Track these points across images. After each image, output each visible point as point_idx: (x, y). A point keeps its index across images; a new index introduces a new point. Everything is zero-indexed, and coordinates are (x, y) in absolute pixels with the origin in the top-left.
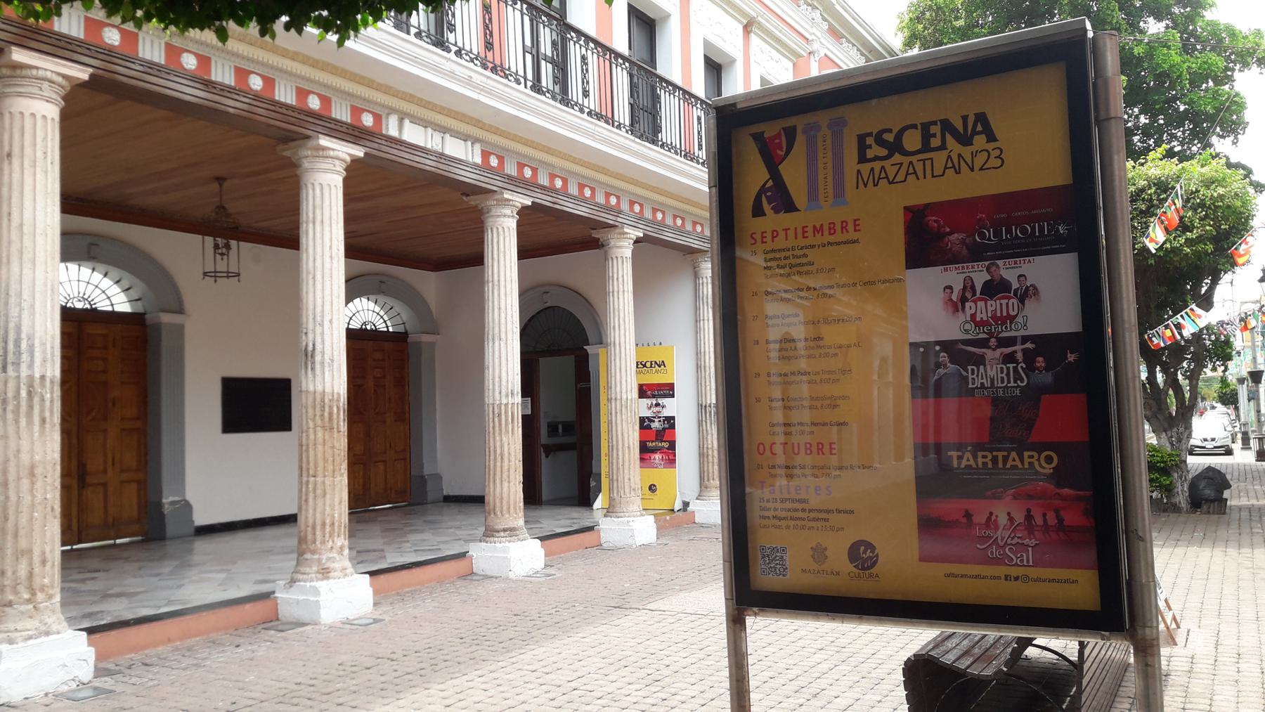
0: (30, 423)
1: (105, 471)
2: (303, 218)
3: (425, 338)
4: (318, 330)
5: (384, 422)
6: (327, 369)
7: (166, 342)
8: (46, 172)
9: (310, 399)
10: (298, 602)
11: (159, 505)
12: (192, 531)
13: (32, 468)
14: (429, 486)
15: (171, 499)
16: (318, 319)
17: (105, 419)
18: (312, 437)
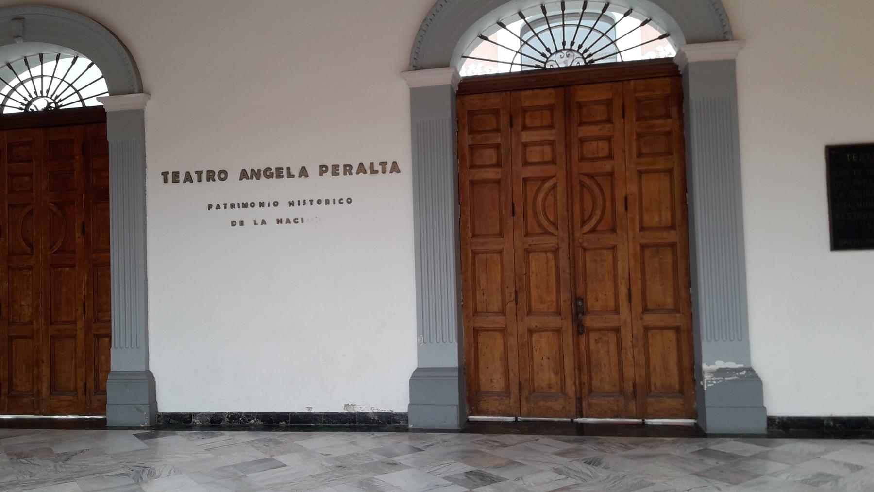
1: (617, 311)
12: (762, 427)
15: (720, 364)
17: (613, 230)
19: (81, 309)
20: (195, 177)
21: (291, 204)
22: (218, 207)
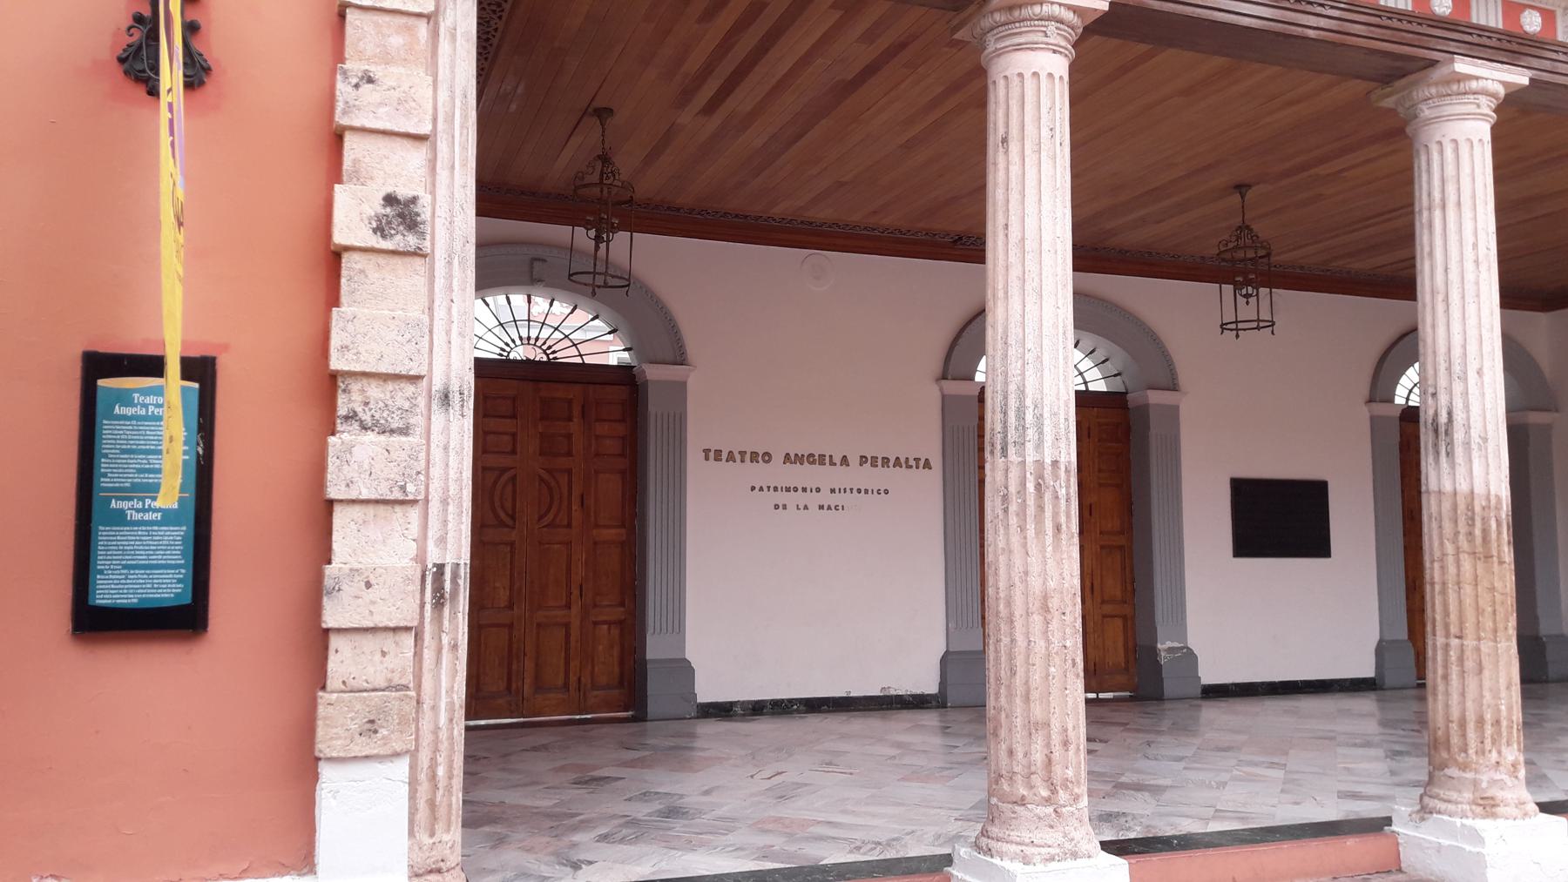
0: (1040, 532)
2: (1422, 200)
4: (1458, 388)
6: (1475, 454)
7: (1156, 430)
8: (1054, 158)
9: (1447, 506)
10: (1439, 849)
11: (1153, 651)
13: (1045, 597)
15: (1169, 644)
16: (1457, 368)
18: (1452, 569)
19: (576, 592)
20: (738, 457)
21: (833, 491)
22: (761, 489)
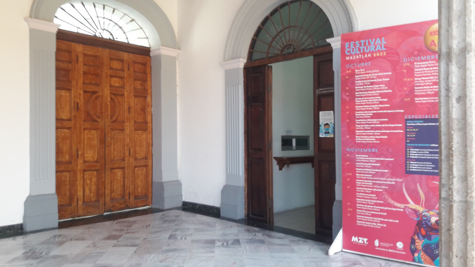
3: (166, 52)
5: (123, 130)
14: (167, 193)
